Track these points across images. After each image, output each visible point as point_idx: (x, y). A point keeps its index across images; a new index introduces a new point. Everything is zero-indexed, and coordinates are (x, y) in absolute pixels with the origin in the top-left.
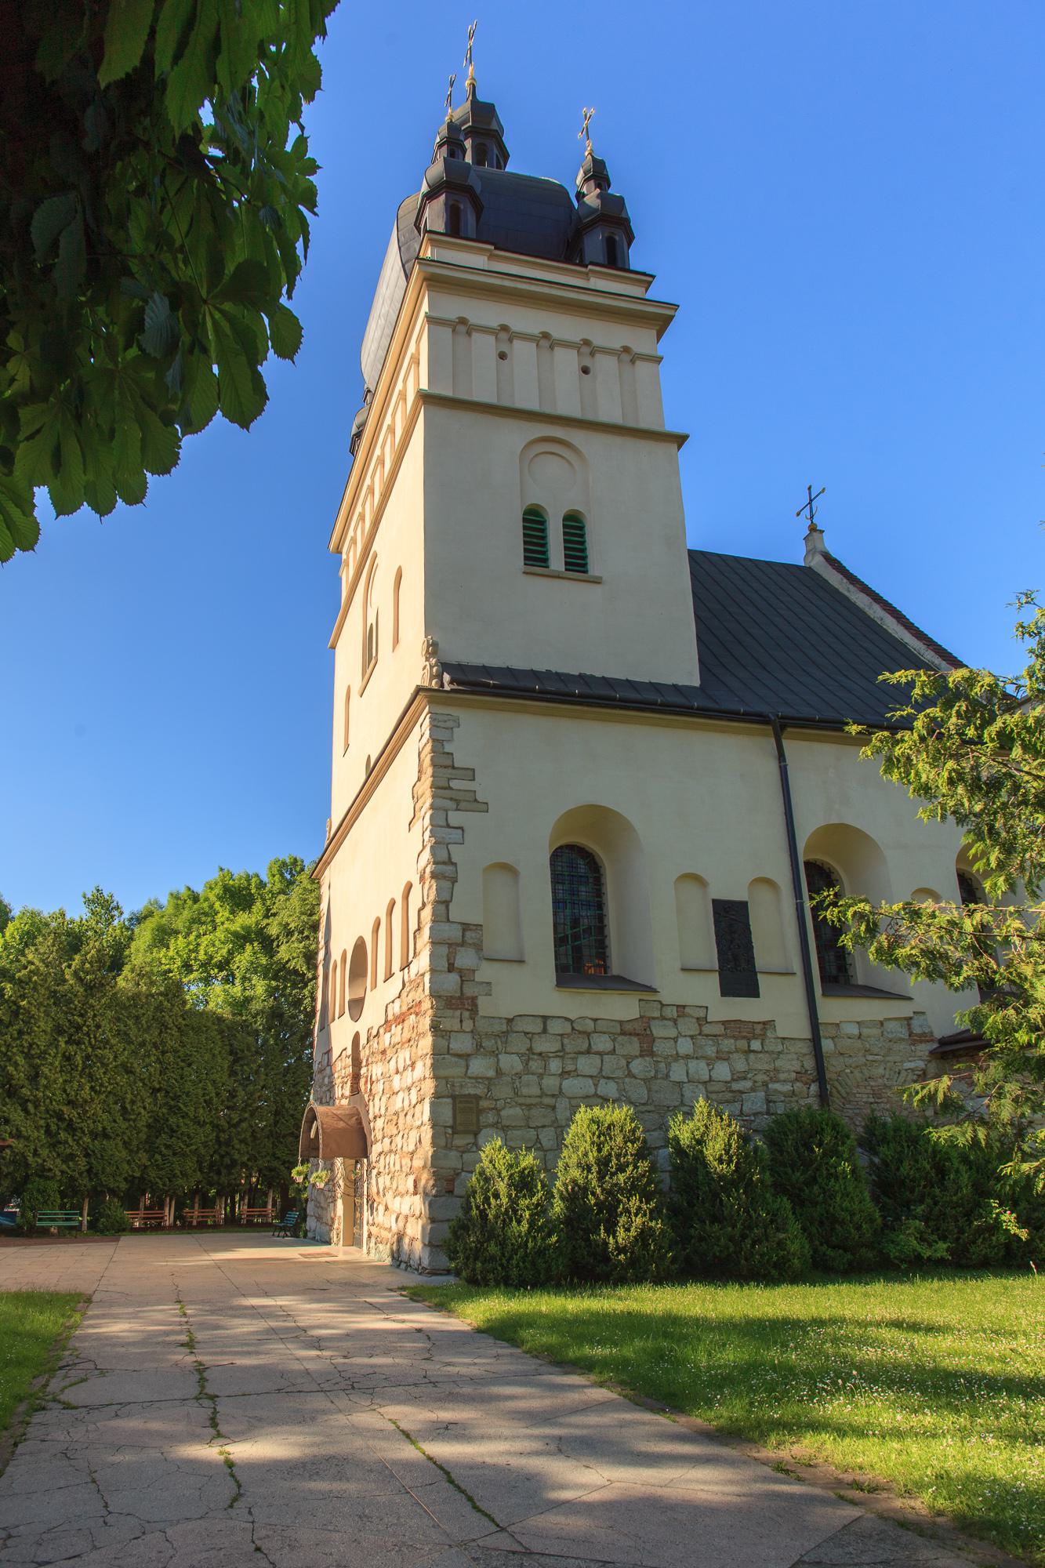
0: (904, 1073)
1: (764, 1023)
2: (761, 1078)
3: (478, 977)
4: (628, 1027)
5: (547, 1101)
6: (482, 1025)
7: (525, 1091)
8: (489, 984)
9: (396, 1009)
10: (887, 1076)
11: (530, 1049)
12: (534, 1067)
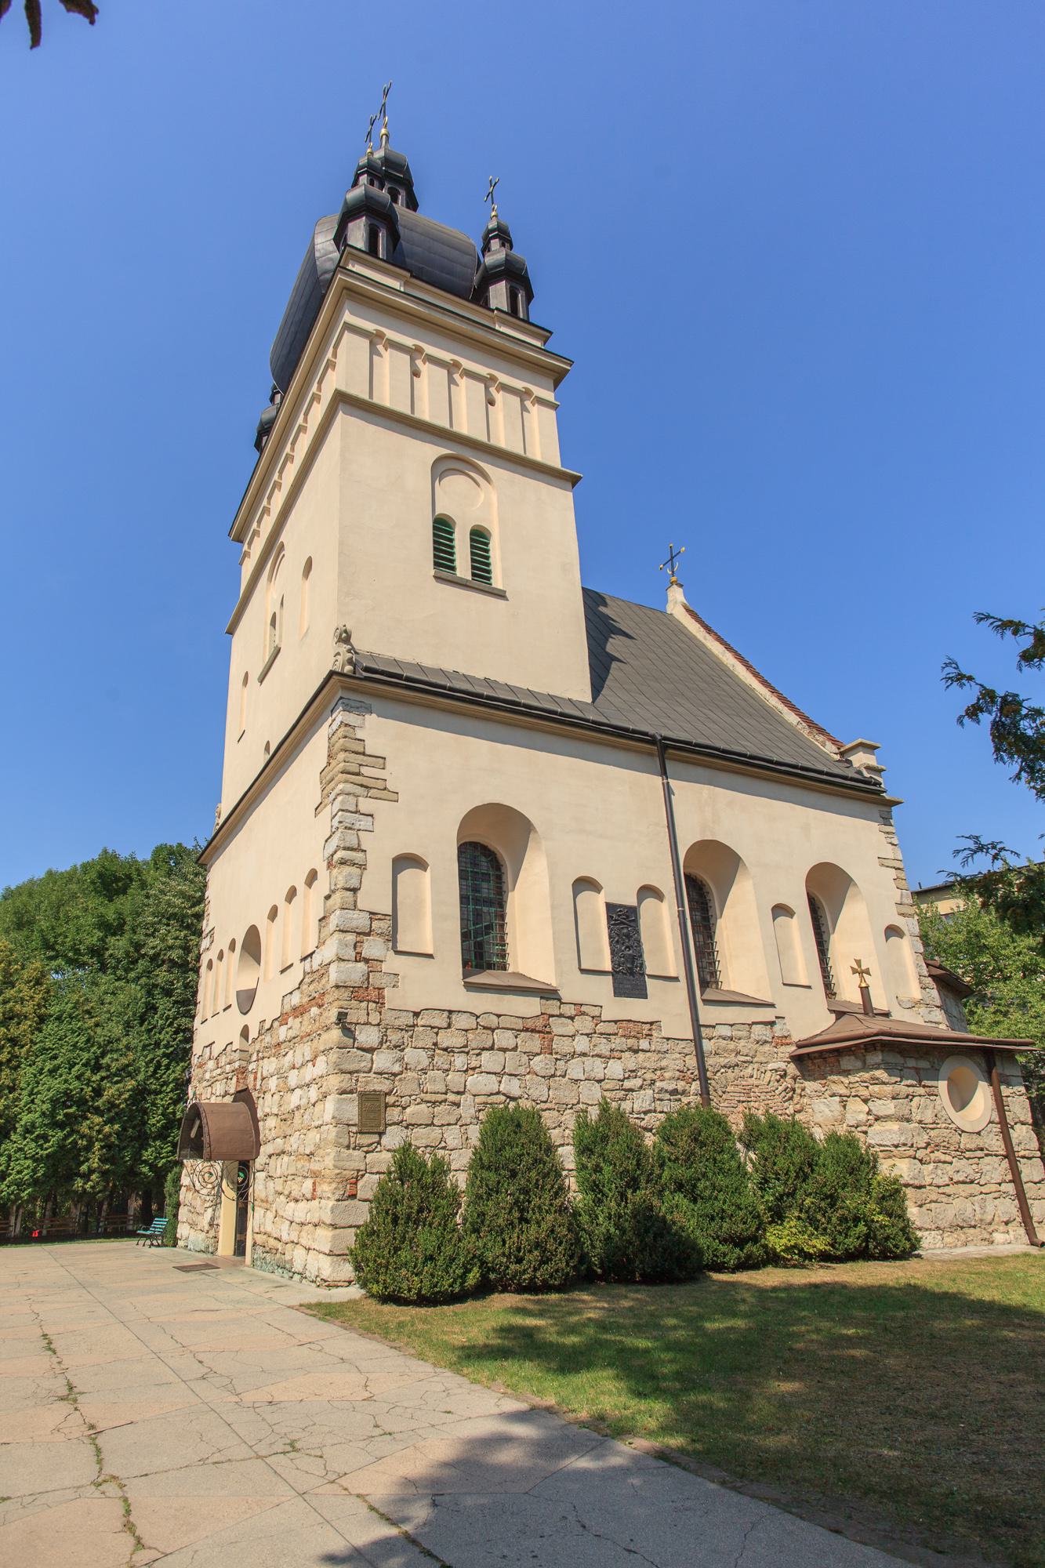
0: (769, 1074)
1: (652, 1023)
2: (649, 1076)
3: (385, 967)
4: (530, 1024)
5: (451, 1097)
6: (388, 1017)
7: (429, 1087)
9: (296, 999)
10: (755, 1076)
11: (435, 1044)
12: (440, 1063)
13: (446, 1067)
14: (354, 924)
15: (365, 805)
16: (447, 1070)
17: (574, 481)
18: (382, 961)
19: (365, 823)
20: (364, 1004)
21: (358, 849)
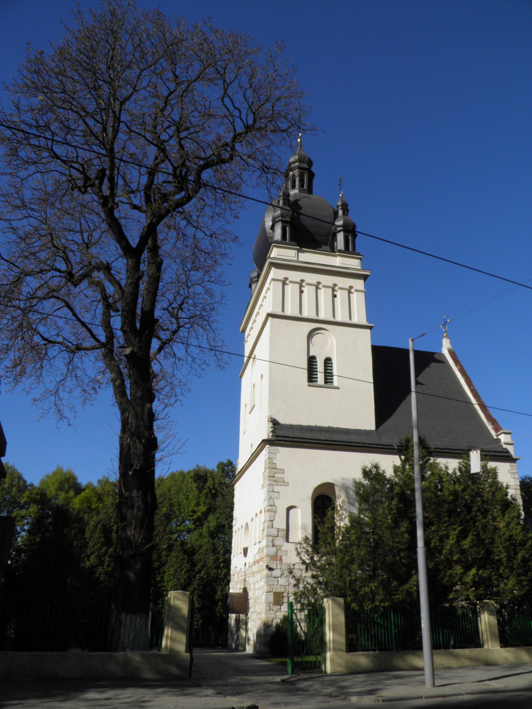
3: (283, 549)
8: (287, 551)
14: (272, 533)
15: (276, 488)
17: (371, 328)
19: (276, 495)
20: (275, 562)
21: (274, 505)
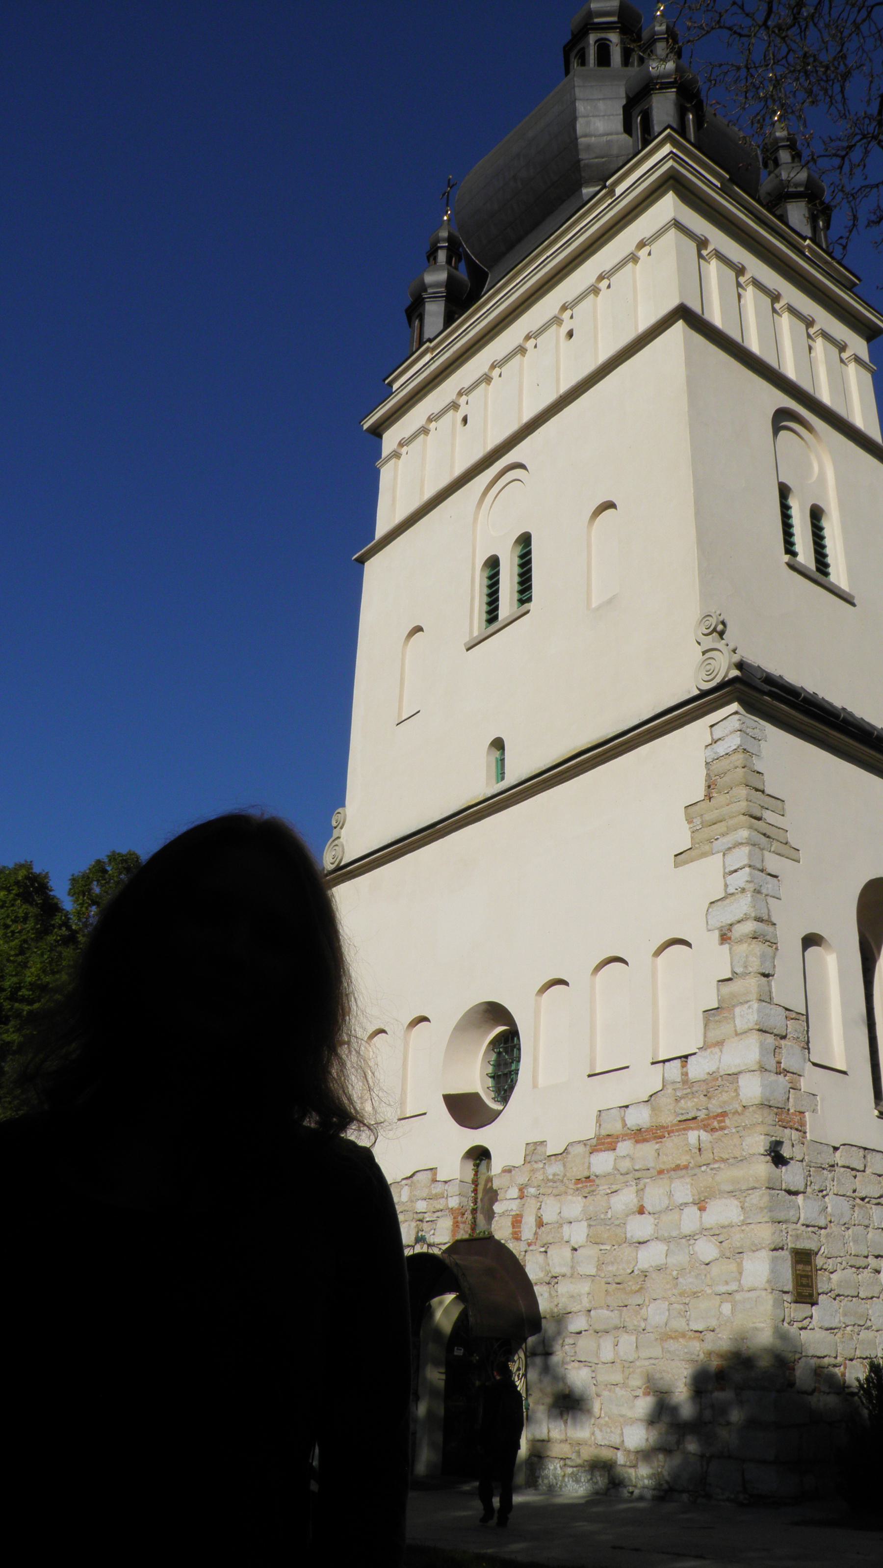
13: (866, 1222)
16: (867, 1227)
18: (800, 1076)
